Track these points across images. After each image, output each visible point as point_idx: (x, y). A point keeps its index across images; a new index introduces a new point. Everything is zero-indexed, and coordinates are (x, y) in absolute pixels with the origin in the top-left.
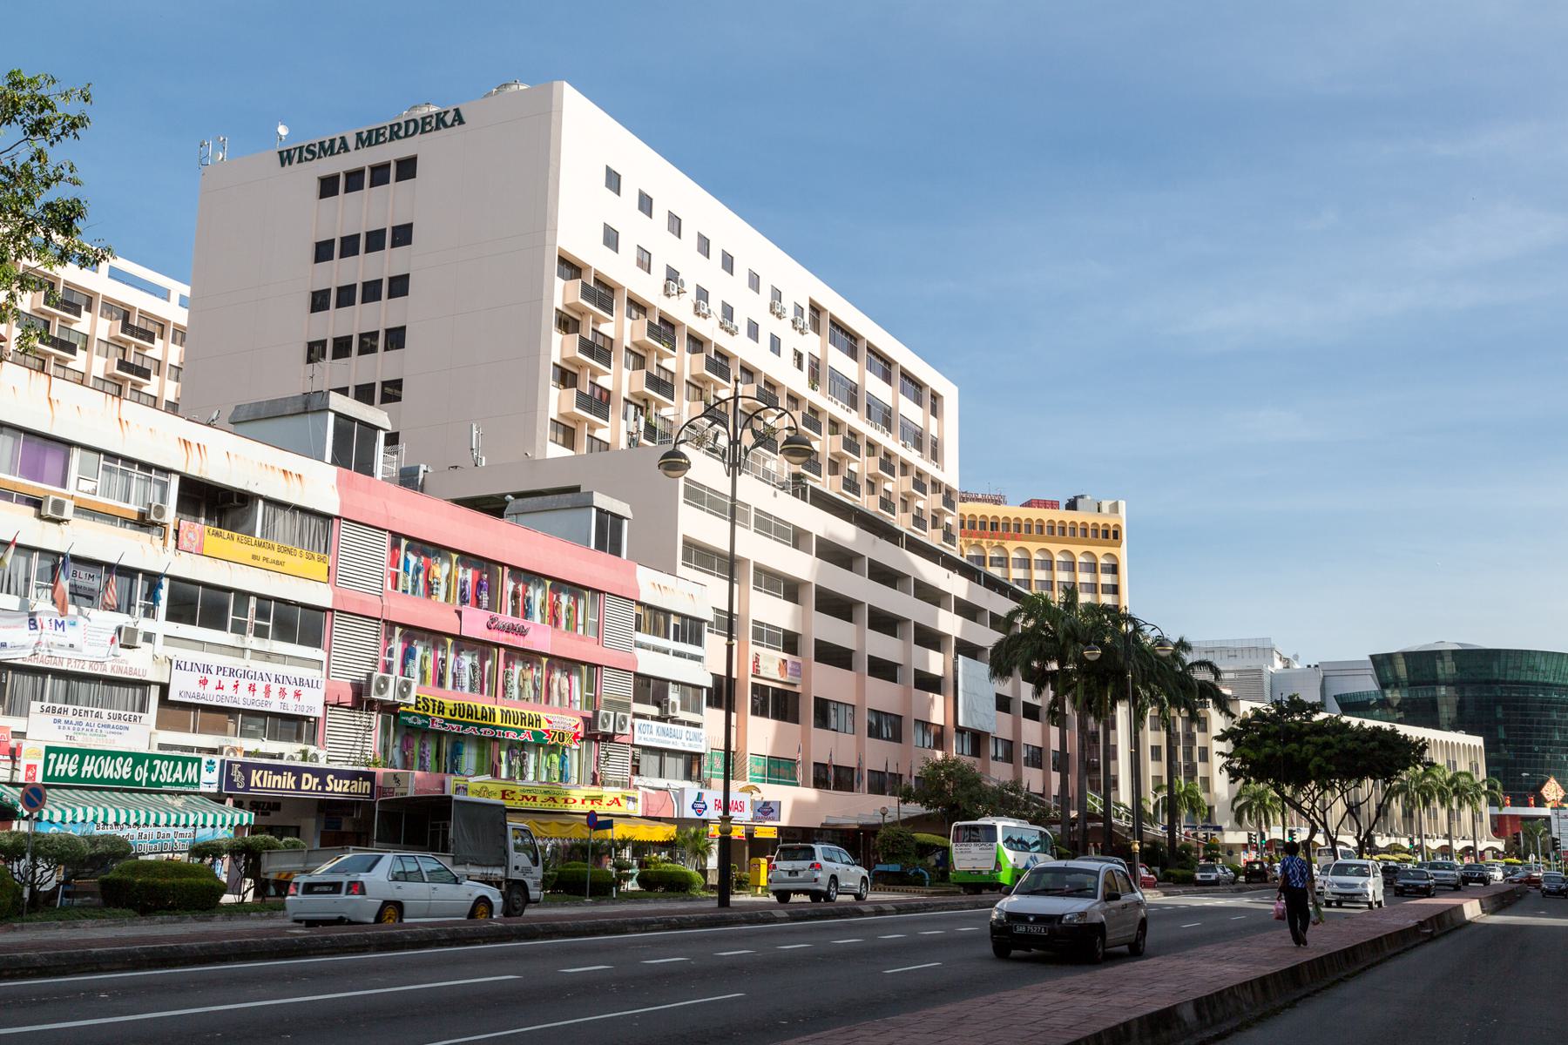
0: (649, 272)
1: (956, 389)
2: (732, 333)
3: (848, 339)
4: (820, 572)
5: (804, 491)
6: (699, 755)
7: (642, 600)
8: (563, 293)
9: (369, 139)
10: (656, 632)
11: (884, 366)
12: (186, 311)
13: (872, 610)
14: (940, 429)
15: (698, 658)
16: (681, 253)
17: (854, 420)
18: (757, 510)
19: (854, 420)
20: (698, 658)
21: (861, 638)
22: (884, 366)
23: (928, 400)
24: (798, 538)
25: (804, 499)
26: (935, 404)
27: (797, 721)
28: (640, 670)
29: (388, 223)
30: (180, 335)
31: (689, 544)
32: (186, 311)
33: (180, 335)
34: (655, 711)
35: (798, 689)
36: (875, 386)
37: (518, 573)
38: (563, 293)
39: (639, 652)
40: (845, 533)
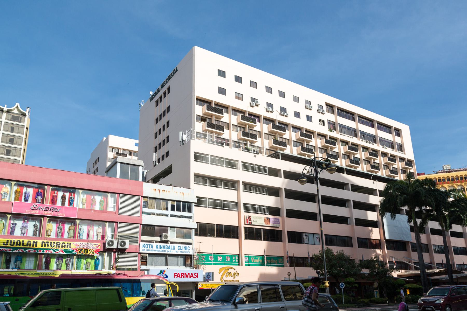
0: (242, 100)
1: (408, 126)
2: (287, 117)
3: (343, 112)
4: (368, 199)
5: (279, 155)
6: (190, 256)
7: (144, 195)
8: (199, 110)
9: (162, 87)
10: (184, 210)
11: (370, 122)
12: (138, 147)
13: (354, 202)
14: (402, 141)
15: (190, 217)
16: (274, 99)
17: (389, 151)
18: (242, 162)
19: (389, 151)
20: (190, 217)
21: (351, 212)
22: (370, 122)
23: (394, 131)
24: (274, 172)
25: (279, 158)
26: (398, 132)
27: (282, 241)
28: (143, 223)
29: (166, 108)
30: (136, 153)
31: (196, 176)
32: (138, 147)
33: (136, 153)
34: (158, 239)
35: (280, 229)
36: (382, 134)
37: (57, 188)
38: (199, 110)
39: (144, 216)
40: (299, 168)
